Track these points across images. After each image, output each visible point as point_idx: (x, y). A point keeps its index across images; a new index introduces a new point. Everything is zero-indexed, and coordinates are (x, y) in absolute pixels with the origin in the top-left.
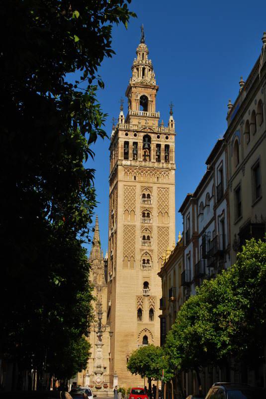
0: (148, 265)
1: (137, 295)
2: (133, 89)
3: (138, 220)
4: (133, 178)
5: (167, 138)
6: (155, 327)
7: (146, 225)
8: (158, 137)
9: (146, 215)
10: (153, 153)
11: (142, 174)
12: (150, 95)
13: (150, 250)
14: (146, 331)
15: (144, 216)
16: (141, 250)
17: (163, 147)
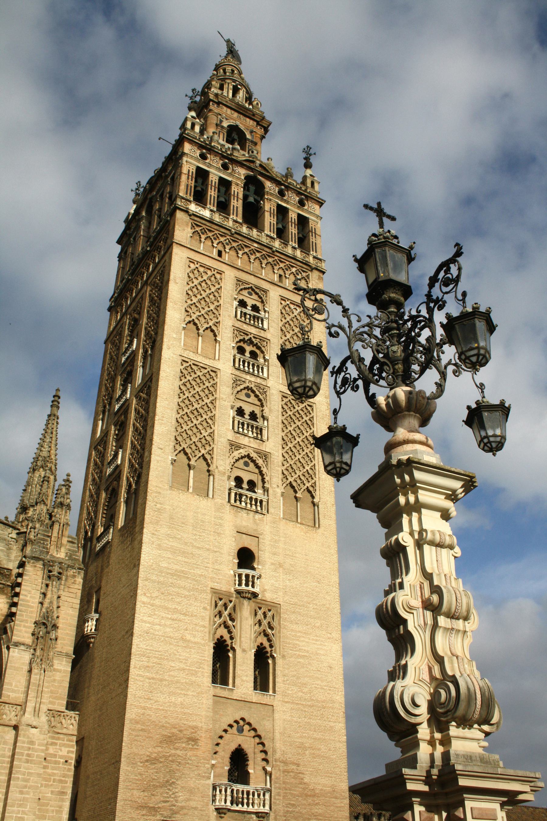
0: (250, 494)
1: (217, 586)
2: (212, 106)
3: (224, 360)
4: (215, 252)
5: (301, 203)
6: (277, 716)
7: (248, 377)
8: (281, 193)
9: (247, 354)
10: (269, 220)
11: (240, 253)
12: (252, 132)
13: (259, 452)
14: (240, 730)
15: (241, 350)
16: (232, 445)
17: (293, 216)
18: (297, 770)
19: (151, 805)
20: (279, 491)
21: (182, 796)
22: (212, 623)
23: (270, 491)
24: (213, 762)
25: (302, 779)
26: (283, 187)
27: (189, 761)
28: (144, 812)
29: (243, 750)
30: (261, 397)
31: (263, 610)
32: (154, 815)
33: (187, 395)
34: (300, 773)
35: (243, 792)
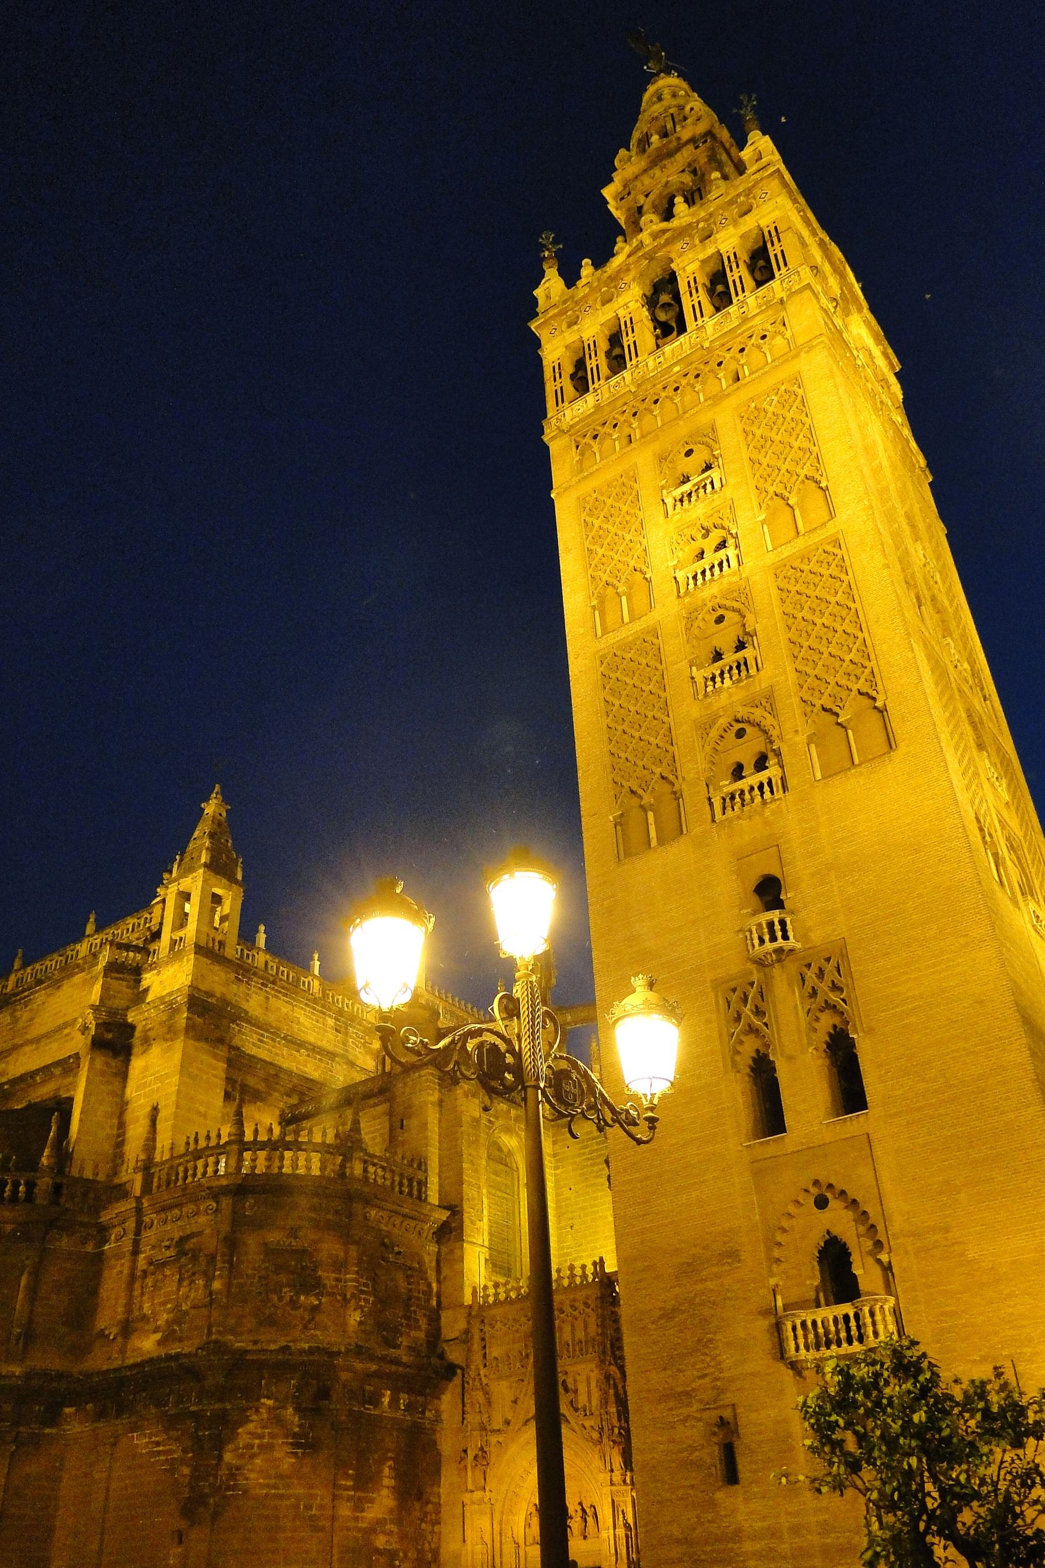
18: (947, 1239)
19: (680, 1389)
20: (801, 739)
21: (727, 1359)
22: (726, 1038)
23: (784, 751)
24: (773, 1281)
25: (962, 1255)
26: (702, 225)
27: (729, 1295)
28: (671, 1404)
29: (836, 1237)
30: (736, 605)
31: (814, 968)
32: (687, 1406)
33: (617, 703)
34: (953, 1244)
35: (814, 1323)
